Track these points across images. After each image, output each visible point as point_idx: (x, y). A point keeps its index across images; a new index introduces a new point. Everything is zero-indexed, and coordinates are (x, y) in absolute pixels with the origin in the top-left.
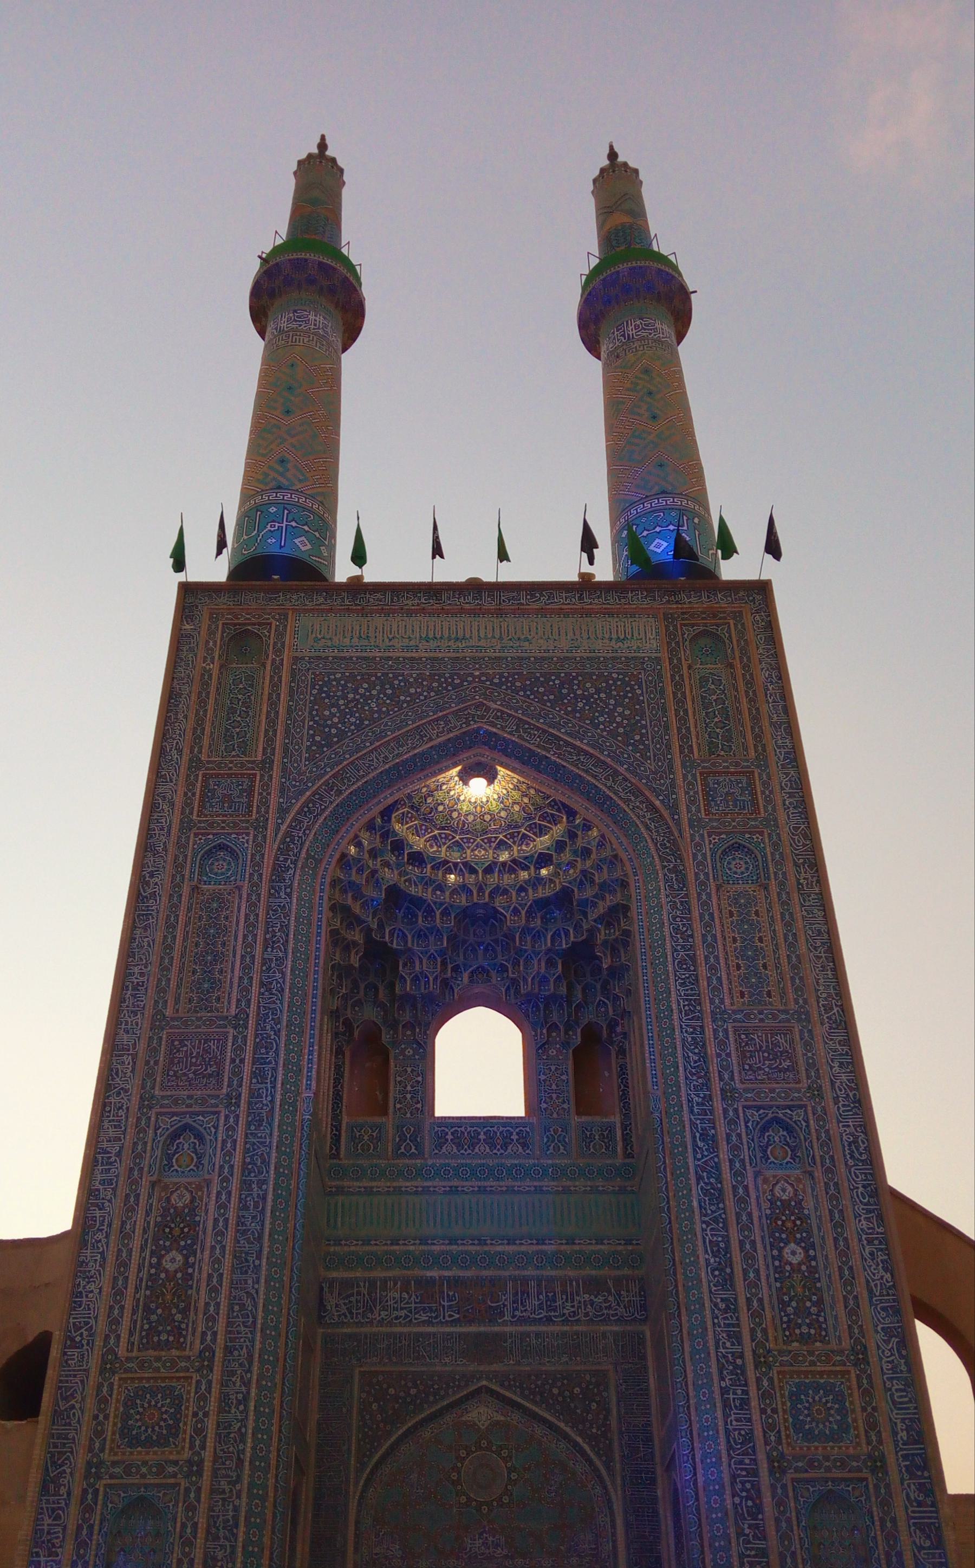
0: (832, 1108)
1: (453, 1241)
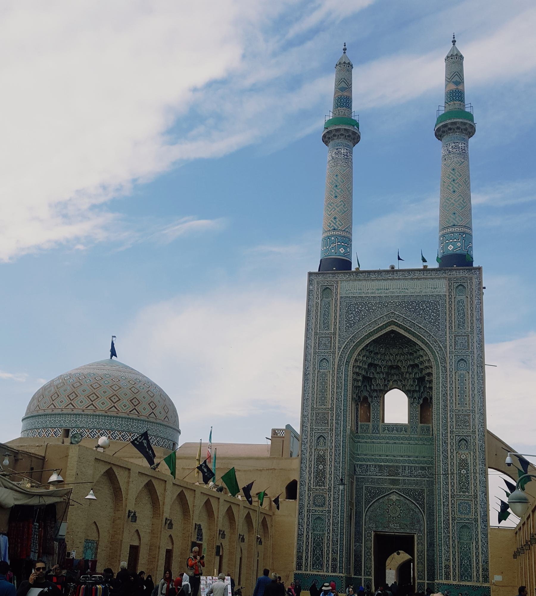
0: (477, 437)
1: (387, 456)
